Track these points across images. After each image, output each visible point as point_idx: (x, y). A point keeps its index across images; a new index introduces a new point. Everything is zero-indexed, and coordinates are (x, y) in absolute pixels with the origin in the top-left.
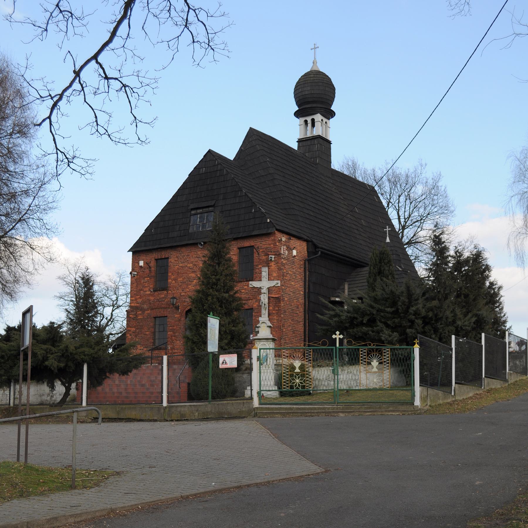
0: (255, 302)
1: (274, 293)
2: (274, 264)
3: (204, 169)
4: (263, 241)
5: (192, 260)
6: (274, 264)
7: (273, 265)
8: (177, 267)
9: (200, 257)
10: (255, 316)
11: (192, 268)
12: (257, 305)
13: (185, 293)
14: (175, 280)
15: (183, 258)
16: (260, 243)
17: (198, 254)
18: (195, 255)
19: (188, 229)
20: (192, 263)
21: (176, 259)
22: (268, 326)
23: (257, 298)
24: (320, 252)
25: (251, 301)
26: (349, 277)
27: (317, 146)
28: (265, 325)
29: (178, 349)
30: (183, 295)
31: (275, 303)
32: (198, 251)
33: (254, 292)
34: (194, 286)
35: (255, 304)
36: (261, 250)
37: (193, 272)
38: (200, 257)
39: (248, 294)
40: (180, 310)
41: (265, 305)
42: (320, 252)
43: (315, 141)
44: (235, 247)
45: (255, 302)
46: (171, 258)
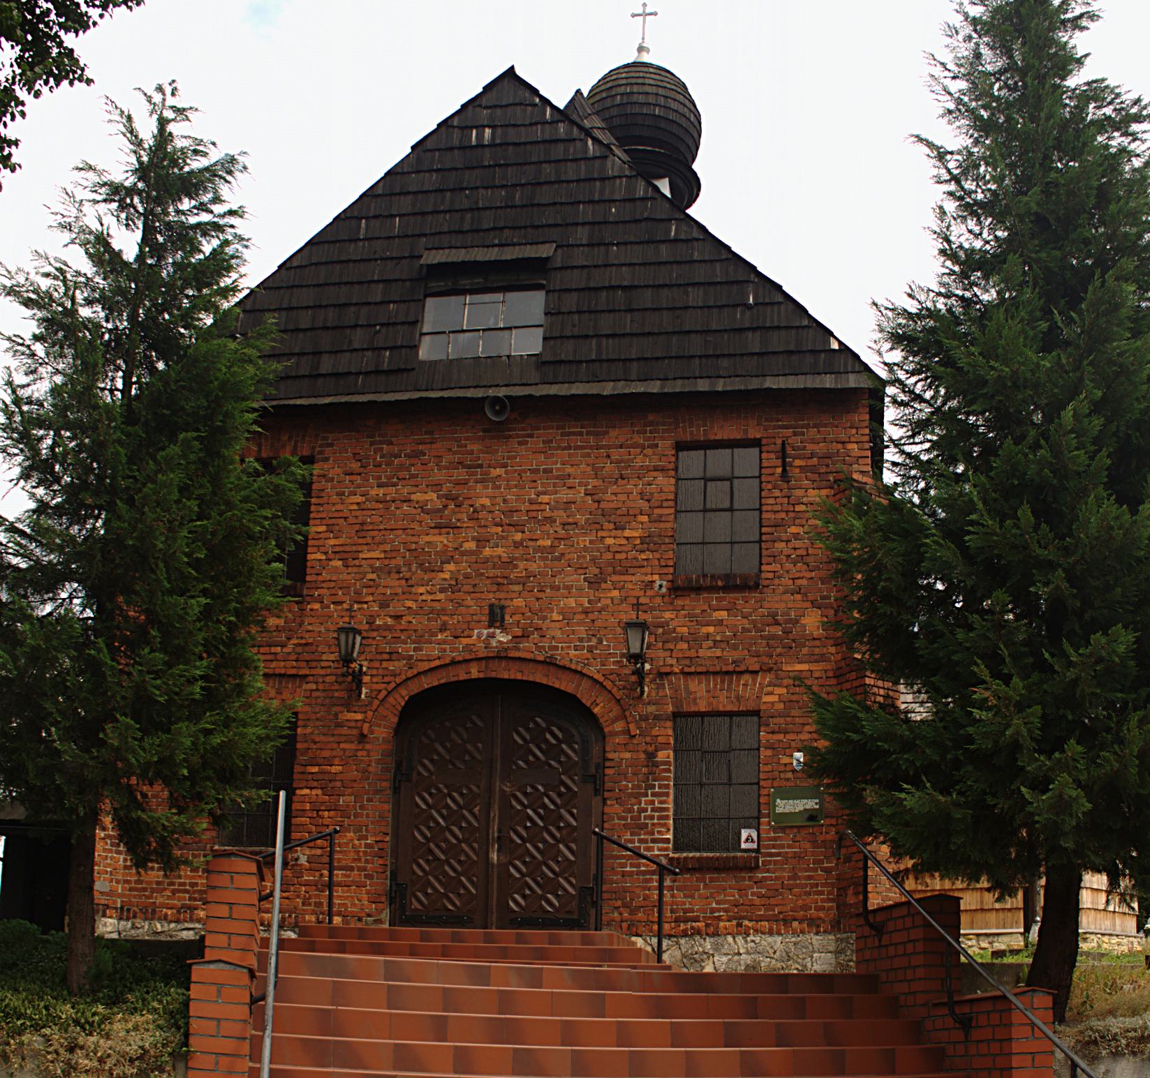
3: (488, 131)
4: (808, 426)
5: (439, 475)
8: (359, 499)
9: (481, 466)
10: (770, 747)
11: (438, 510)
13: (398, 617)
14: (347, 556)
15: (388, 464)
16: (795, 434)
17: (472, 452)
18: (456, 453)
19: (415, 348)
20: (436, 486)
21: (355, 466)
29: (352, 869)
30: (387, 628)
32: (467, 439)
34: (442, 590)
35: (771, 693)
36: (798, 462)
37: (438, 527)
38: (481, 466)
40: (364, 690)
44: (663, 438)
46: (327, 459)
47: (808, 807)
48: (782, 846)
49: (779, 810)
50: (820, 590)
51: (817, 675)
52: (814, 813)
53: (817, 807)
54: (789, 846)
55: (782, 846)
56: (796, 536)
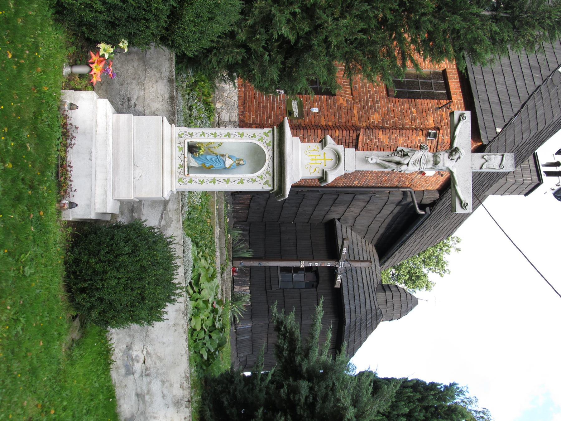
0: (347, 100)
1: (366, 140)
2: (419, 140)
6: (419, 140)
7: (419, 138)
10: (320, 99)
12: (341, 104)
22: (325, 173)
23: (354, 104)
24: (423, 213)
25: (349, 91)
26: (367, 242)
27: (529, 180)
28: (330, 163)
31: (347, 141)
33: (367, 98)
35: (343, 100)
39: (363, 87)
41: (398, 163)
42: (423, 213)
43: (535, 177)
45: (347, 100)
47: (295, 113)
48: (277, 103)
49: (293, 102)
50: (390, 121)
51: (353, 118)
52: (292, 115)
53: (295, 116)
54: (277, 106)
55: (277, 103)
56: (412, 113)
